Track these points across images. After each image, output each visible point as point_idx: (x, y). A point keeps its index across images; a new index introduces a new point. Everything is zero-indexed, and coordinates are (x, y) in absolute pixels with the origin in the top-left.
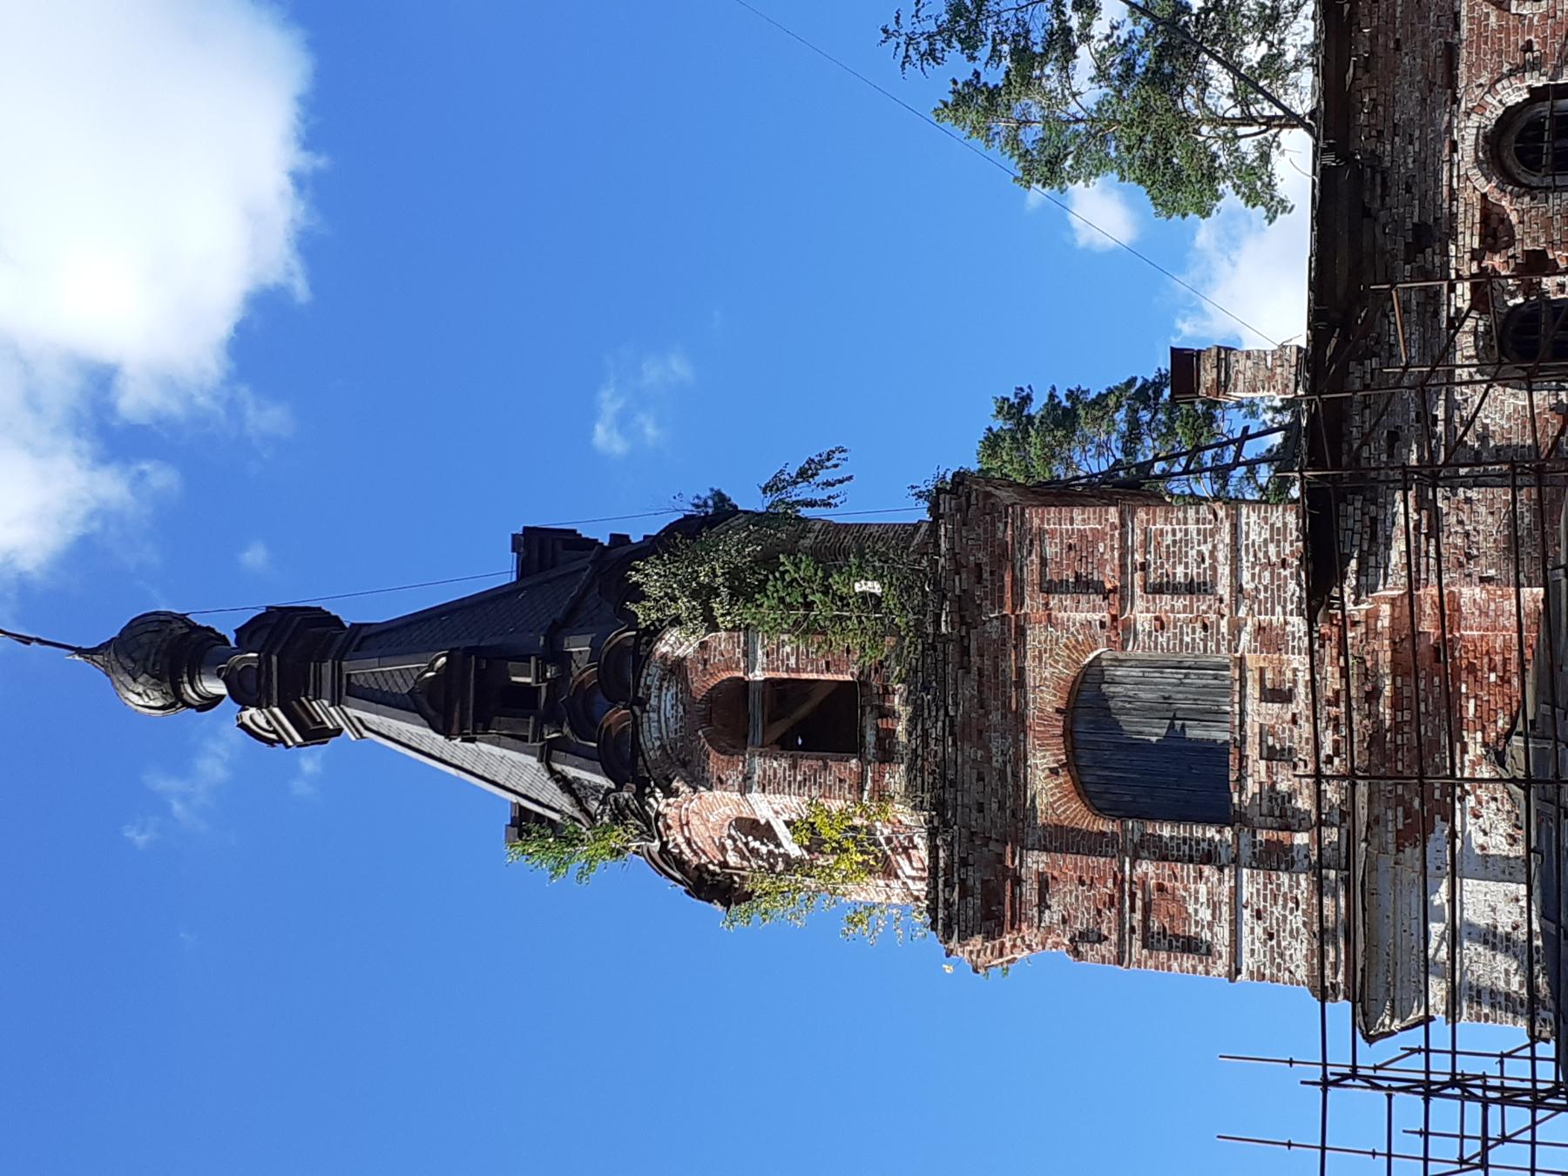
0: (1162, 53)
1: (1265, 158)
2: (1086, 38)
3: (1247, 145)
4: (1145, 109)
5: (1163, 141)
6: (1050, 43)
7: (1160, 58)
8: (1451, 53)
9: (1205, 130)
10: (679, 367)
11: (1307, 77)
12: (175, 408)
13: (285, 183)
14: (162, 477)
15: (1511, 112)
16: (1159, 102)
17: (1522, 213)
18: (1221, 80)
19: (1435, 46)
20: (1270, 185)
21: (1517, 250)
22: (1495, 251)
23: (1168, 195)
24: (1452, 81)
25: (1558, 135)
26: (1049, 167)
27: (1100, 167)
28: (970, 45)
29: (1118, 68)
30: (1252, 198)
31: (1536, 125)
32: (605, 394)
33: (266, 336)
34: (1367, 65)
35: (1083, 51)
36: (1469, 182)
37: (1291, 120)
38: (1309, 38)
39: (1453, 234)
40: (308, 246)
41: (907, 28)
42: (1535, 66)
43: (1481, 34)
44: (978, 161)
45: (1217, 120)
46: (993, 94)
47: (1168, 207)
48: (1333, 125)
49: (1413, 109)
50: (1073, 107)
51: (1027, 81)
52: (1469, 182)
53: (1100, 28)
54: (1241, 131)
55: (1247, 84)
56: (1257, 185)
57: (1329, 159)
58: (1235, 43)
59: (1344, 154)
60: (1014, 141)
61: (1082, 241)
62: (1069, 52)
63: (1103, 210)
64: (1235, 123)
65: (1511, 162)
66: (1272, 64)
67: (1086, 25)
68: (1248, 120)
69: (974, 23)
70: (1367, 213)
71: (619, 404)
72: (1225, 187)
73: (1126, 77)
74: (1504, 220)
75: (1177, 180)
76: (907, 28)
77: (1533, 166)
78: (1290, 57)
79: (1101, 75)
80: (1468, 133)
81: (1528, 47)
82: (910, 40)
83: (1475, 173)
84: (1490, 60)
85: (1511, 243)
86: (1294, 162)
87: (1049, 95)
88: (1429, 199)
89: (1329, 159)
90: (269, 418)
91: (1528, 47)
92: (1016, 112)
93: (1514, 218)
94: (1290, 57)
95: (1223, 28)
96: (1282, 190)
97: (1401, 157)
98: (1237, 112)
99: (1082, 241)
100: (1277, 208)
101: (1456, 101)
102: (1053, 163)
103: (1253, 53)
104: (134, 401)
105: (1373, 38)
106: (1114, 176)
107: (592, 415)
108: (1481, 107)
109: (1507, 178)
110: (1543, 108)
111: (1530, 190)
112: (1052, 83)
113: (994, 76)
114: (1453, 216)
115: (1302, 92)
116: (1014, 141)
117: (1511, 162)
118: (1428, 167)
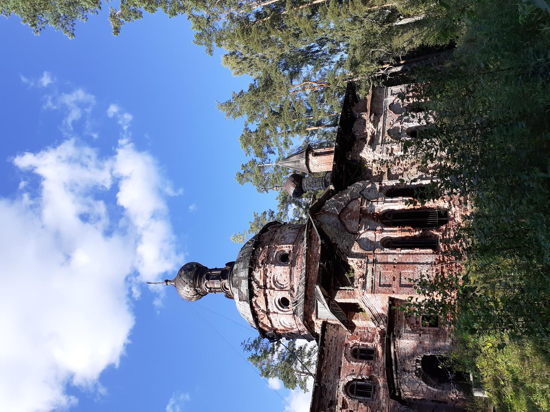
0: (290, 356)
1: (305, 380)
2: (277, 351)
3: (302, 377)
4: (285, 366)
5: (288, 373)
6: (270, 351)
7: (289, 357)
8: (340, 368)
9: (295, 373)
10: (188, 397)
11: (314, 367)
12: (84, 385)
13: (122, 344)
14: (74, 400)
15: (349, 382)
16: (288, 366)
17: (350, 402)
18: (300, 364)
19: (337, 367)
20: (305, 386)
21: (348, 409)
22: (344, 409)
23: (287, 384)
24: (339, 374)
25: (357, 388)
26: (267, 374)
27: (276, 375)
28: (256, 348)
29: (282, 357)
30: (302, 388)
31: (353, 385)
32: (171, 400)
33: (108, 375)
34: (325, 368)
35: (276, 353)
36: (341, 394)
37: (311, 374)
38: (316, 360)
39: (337, 404)
40: (122, 358)
41: (246, 343)
42: (354, 374)
43: (345, 367)
44: (254, 370)
45: (298, 371)
46: (259, 357)
47: (287, 386)
48: (318, 377)
49: (332, 378)
50: (273, 363)
51: (265, 357)
52: (341, 394)
53: (280, 349)
54: (302, 374)
55: (304, 366)
56: (303, 386)
57: (317, 384)
58: (302, 358)
59: (319, 384)
60: (261, 367)
61: (270, 387)
62: (274, 353)
63: (275, 383)
64: (301, 372)
65: (348, 392)
66: (309, 362)
67: (277, 348)
68: (303, 372)
69: (258, 344)
70: (322, 396)
71: (173, 402)
72: (298, 384)
73: (283, 359)
74: (346, 403)
75: (289, 381)
76: (246, 343)
77: (352, 393)
78: (312, 362)
79: (279, 358)
80: (342, 384)
81: (353, 371)
82: (246, 346)
83: (342, 392)
84: (347, 371)
85: (347, 408)
86: (311, 382)
87: (269, 360)
88: (333, 396)
89: (317, 384)
90: (102, 390)
91: (353, 371)
92: (262, 361)
93: (348, 403)
94: (312, 362)
95: (301, 354)
96: (307, 387)
97: (329, 386)
98: (301, 370)
99: (270, 387)
100: (306, 391)
101: (340, 378)
102: (267, 373)
103: (306, 360)
104: (76, 381)
105: (327, 363)
106: (278, 378)
107: (167, 403)
108: (344, 380)
109: (348, 395)
110: (355, 383)
111: (351, 398)
112: (270, 358)
113: (259, 354)
114: (337, 400)
115: (313, 369)
116: (261, 367)
117: (348, 392)
118: (334, 390)
